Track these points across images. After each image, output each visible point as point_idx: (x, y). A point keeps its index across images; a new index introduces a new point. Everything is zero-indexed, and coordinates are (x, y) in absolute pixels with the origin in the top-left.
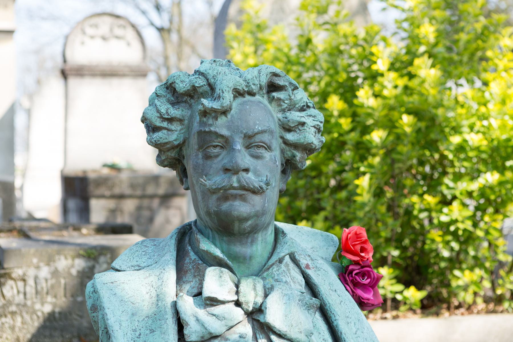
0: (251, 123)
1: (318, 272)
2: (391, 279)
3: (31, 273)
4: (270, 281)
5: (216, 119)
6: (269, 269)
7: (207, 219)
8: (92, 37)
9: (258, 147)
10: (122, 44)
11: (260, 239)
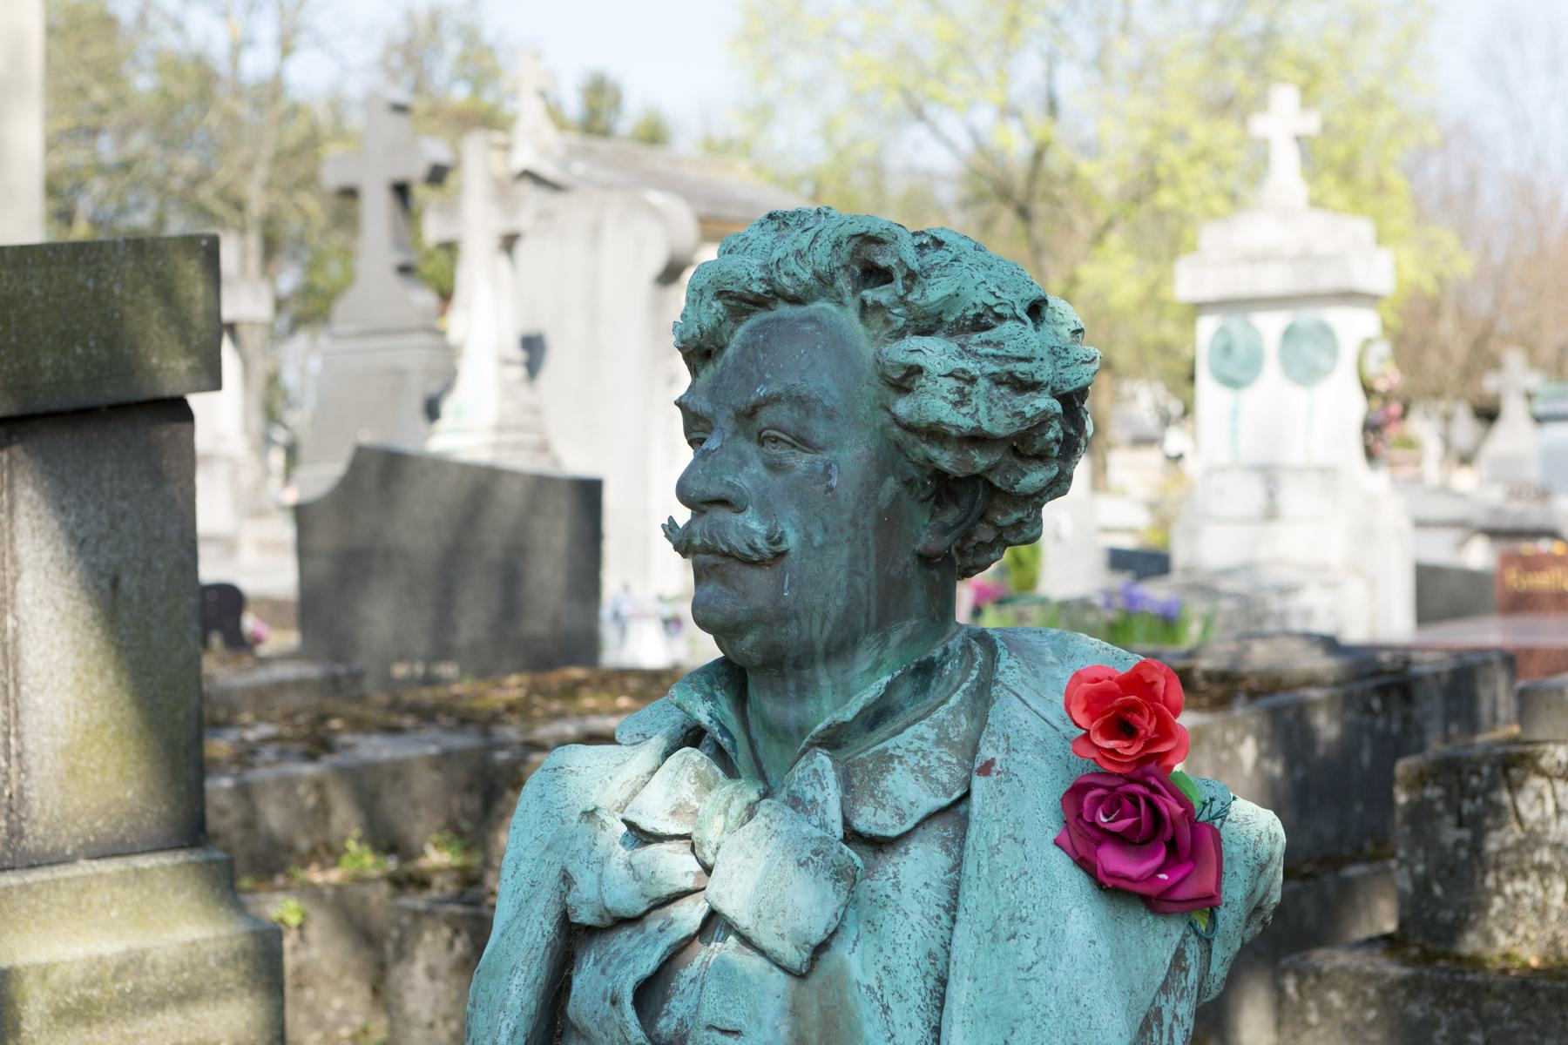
1: (1005, 787)
11: (825, 682)
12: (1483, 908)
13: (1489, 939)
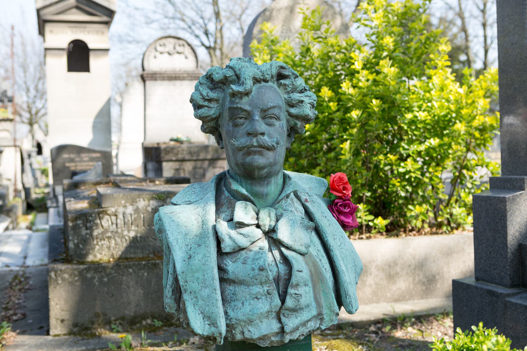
0: (266, 101)
1: (314, 205)
2: (365, 212)
3: (121, 210)
4: (280, 211)
5: (241, 98)
6: (279, 202)
7: (236, 168)
8: (161, 53)
9: (271, 118)
10: (182, 57)
11: (273, 181)
12: (93, 249)
13: (95, 256)
